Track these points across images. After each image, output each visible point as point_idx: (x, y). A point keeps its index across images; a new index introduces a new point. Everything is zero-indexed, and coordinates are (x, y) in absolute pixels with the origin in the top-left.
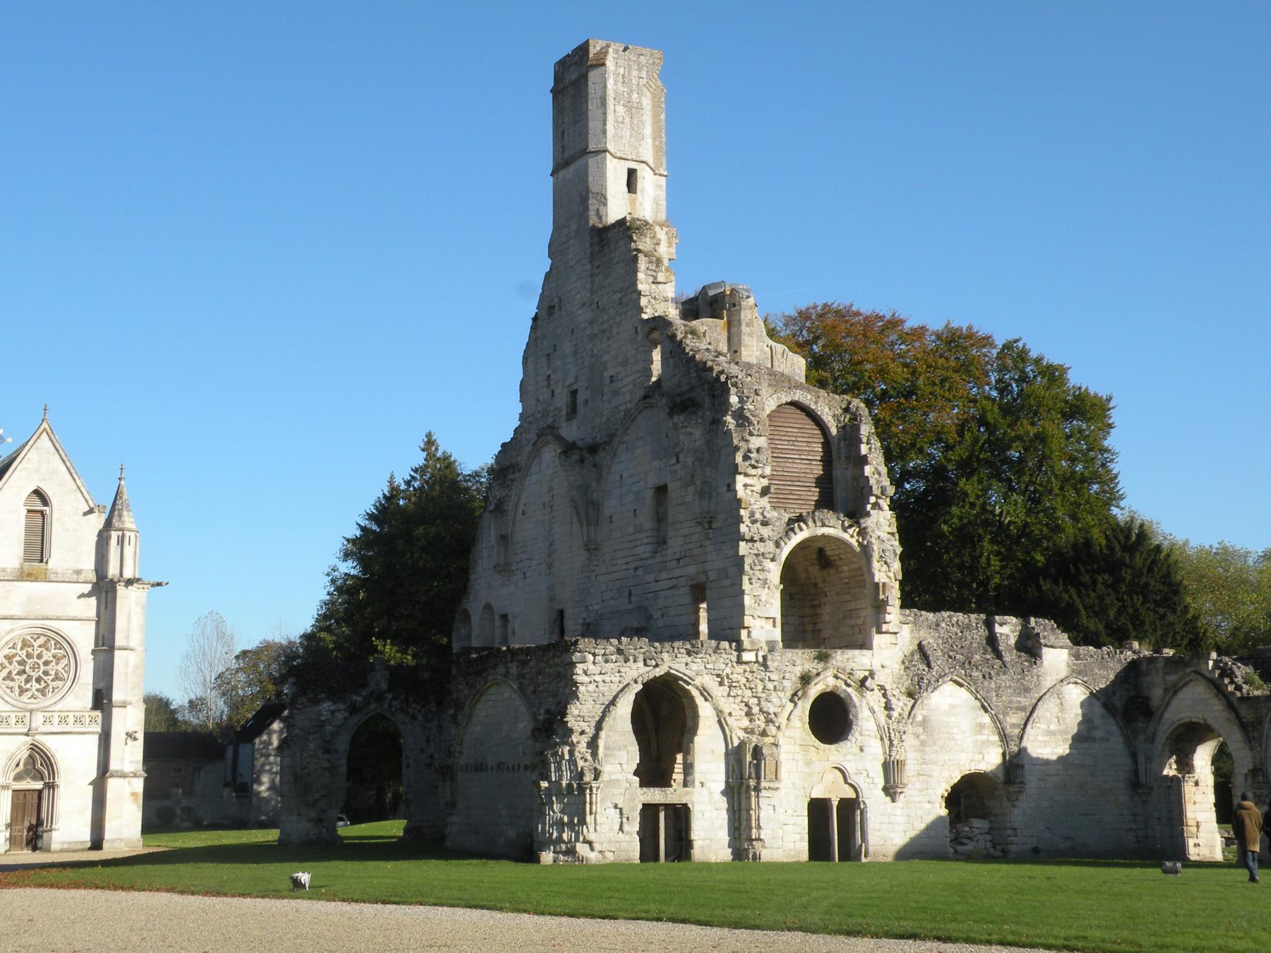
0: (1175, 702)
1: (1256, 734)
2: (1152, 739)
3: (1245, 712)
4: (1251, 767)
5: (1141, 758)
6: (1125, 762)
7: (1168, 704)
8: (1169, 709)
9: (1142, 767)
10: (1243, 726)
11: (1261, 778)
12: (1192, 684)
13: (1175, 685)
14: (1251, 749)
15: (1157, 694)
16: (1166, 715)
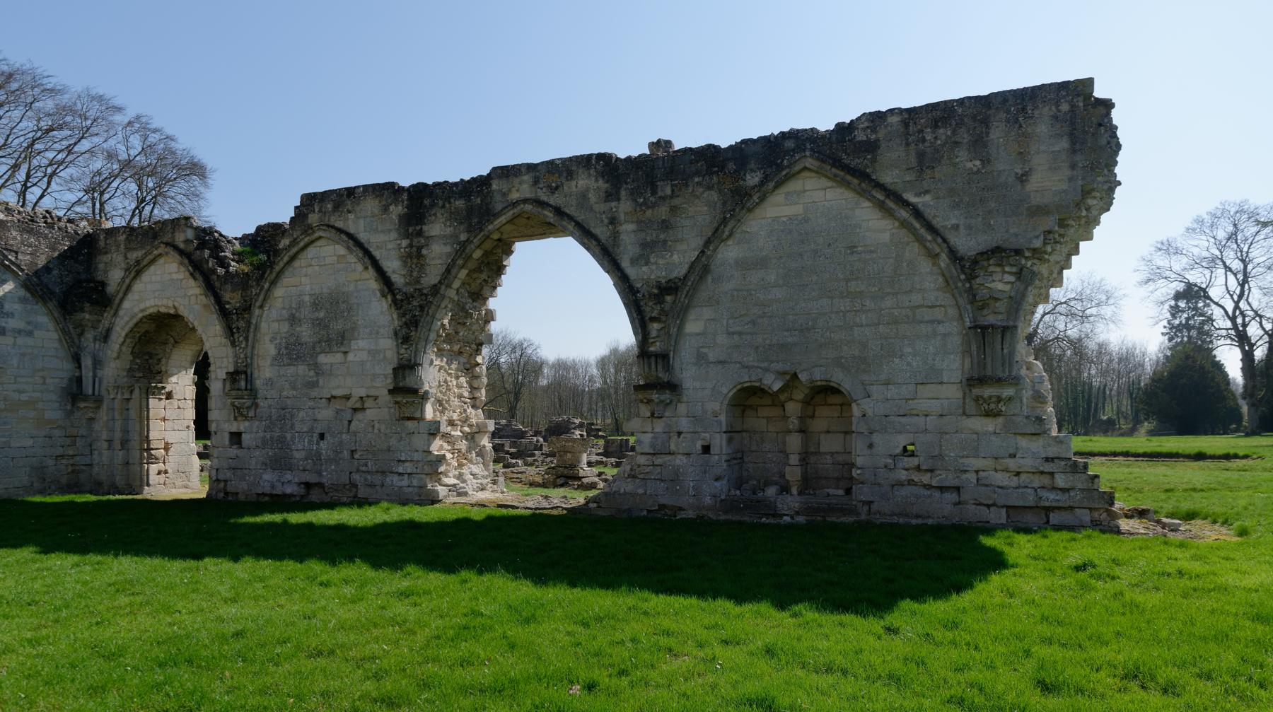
0: (138, 286)
1: (242, 324)
2: (106, 337)
3: (233, 298)
4: (231, 370)
5: (87, 362)
6: (64, 368)
7: (129, 288)
8: (130, 296)
9: (87, 374)
10: (224, 313)
11: (243, 384)
12: (161, 261)
13: (138, 262)
14: (233, 344)
15: (115, 276)
16: (126, 304)
